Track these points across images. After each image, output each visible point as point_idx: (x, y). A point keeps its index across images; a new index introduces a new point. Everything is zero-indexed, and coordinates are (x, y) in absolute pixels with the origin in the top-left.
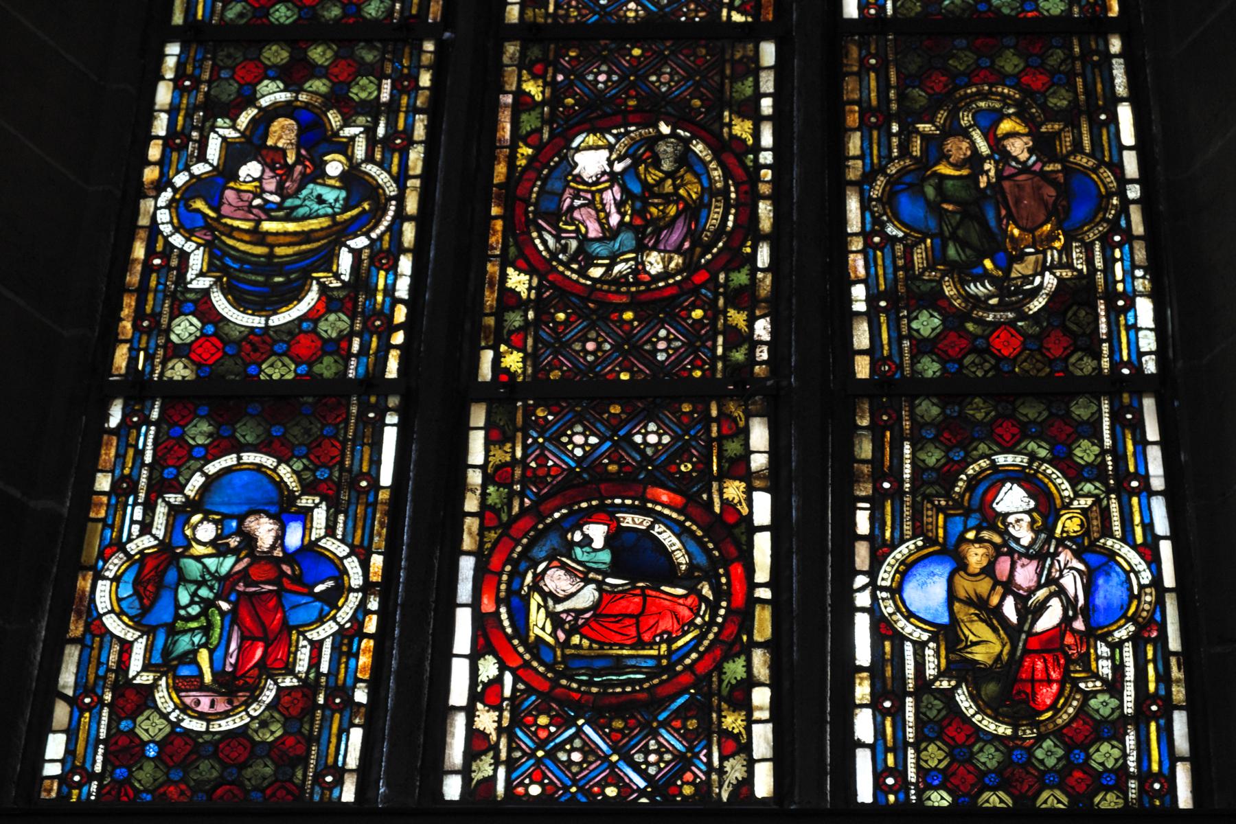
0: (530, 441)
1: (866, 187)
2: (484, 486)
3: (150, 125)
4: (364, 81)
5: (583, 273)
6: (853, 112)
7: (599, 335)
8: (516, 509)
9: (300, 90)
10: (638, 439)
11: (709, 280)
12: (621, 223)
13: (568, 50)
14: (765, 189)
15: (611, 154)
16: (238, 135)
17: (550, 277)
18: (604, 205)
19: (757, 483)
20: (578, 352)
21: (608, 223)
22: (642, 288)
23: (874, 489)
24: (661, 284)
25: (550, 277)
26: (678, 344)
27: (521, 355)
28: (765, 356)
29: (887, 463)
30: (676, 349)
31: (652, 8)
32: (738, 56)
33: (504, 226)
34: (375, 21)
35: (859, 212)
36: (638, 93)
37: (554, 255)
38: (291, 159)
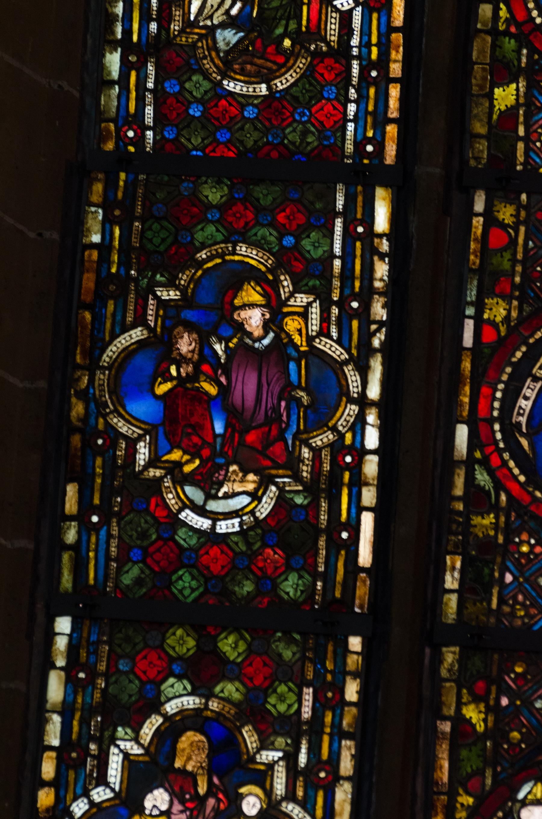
3: (41, 732)
4: (282, 689)
9: (209, 696)
13: (514, 664)
16: (140, 751)
34: (293, 603)
38: (202, 789)
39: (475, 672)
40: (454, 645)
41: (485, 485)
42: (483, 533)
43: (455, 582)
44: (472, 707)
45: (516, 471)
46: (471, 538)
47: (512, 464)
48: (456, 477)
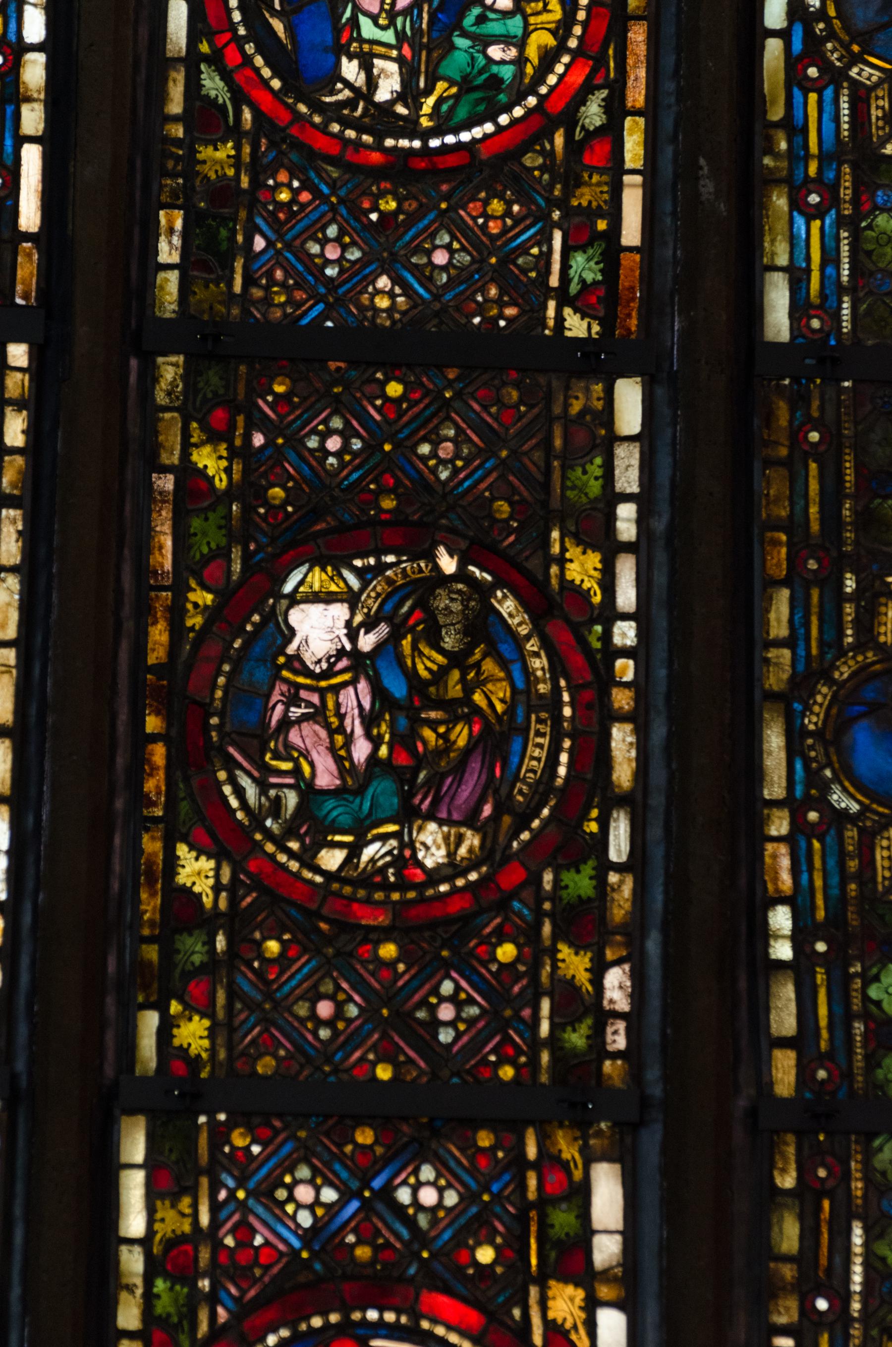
0: (223, 1195)
1: (797, 706)
2: (149, 1278)
5: (308, 859)
6: (777, 543)
7: (338, 988)
8: (204, 1328)
10: (404, 1195)
11: (523, 885)
12: (373, 757)
13: (272, 380)
14: (622, 699)
15: (353, 614)
17: (252, 867)
18: (341, 717)
19: (604, 1292)
20: (302, 1021)
21: (350, 758)
22: (411, 895)
23: (802, 1312)
24: (443, 888)
25: (252, 867)
26: (474, 1011)
27: (206, 1023)
28: (620, 1042)
29: (824, 1261)
30: (471, 1022)
31: (421, 291)
32: (576, 407)
33: (169, 757)
35: (783, 755)
36: (399, 483)
37: (256, 818)
39: (210, 395)
40: (178, 353)
41: (217, 96)
42: (216, 171)
43: (173, 252)
44: (207, 449)
45: (266, 73)
46: (198, 182)
47: (259, 61)
48: (171, 84)
